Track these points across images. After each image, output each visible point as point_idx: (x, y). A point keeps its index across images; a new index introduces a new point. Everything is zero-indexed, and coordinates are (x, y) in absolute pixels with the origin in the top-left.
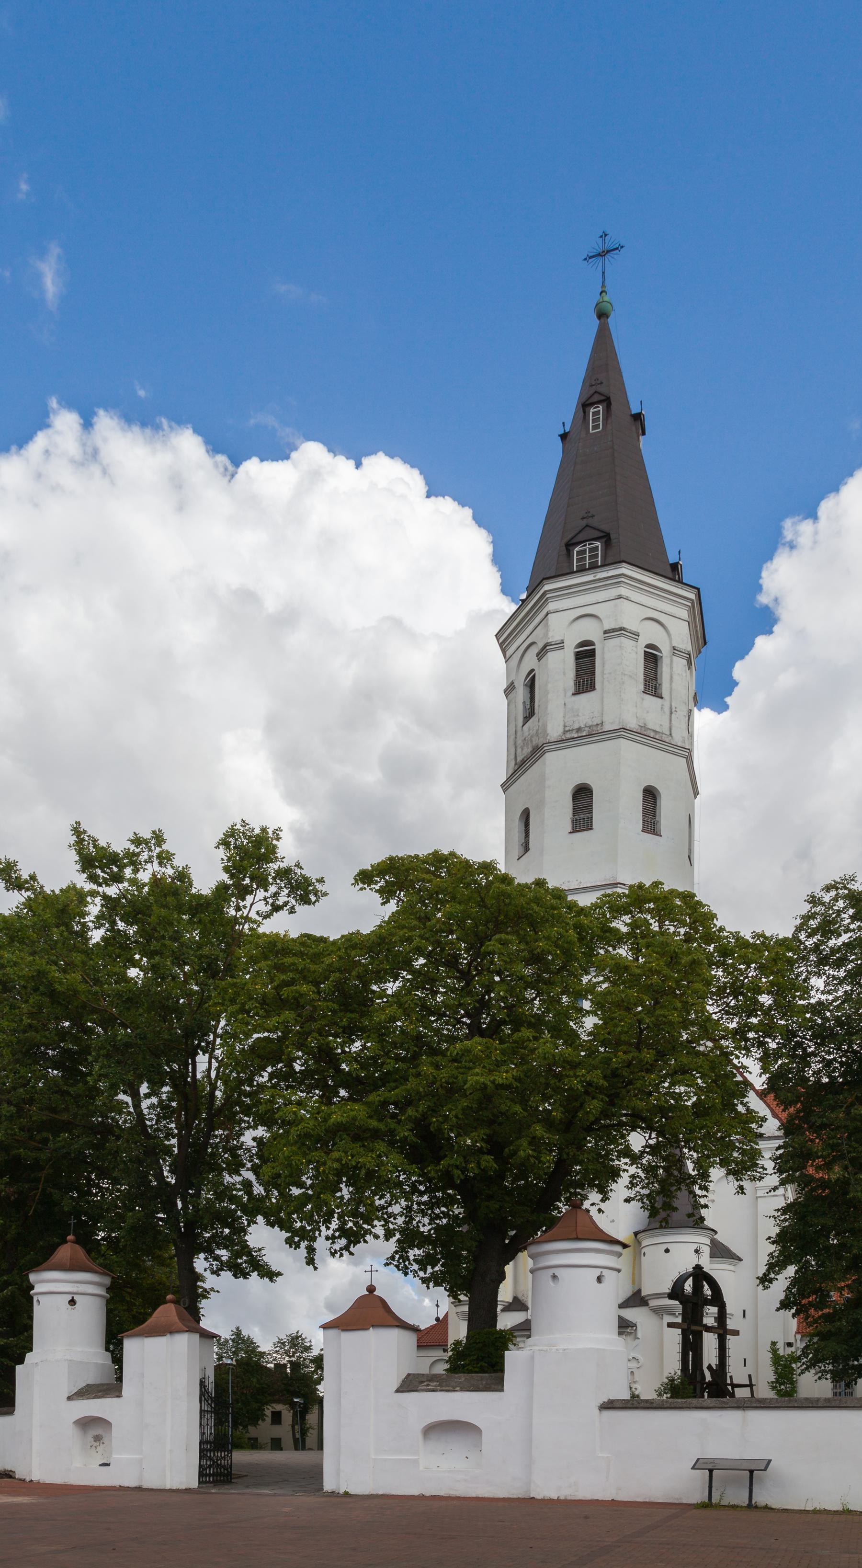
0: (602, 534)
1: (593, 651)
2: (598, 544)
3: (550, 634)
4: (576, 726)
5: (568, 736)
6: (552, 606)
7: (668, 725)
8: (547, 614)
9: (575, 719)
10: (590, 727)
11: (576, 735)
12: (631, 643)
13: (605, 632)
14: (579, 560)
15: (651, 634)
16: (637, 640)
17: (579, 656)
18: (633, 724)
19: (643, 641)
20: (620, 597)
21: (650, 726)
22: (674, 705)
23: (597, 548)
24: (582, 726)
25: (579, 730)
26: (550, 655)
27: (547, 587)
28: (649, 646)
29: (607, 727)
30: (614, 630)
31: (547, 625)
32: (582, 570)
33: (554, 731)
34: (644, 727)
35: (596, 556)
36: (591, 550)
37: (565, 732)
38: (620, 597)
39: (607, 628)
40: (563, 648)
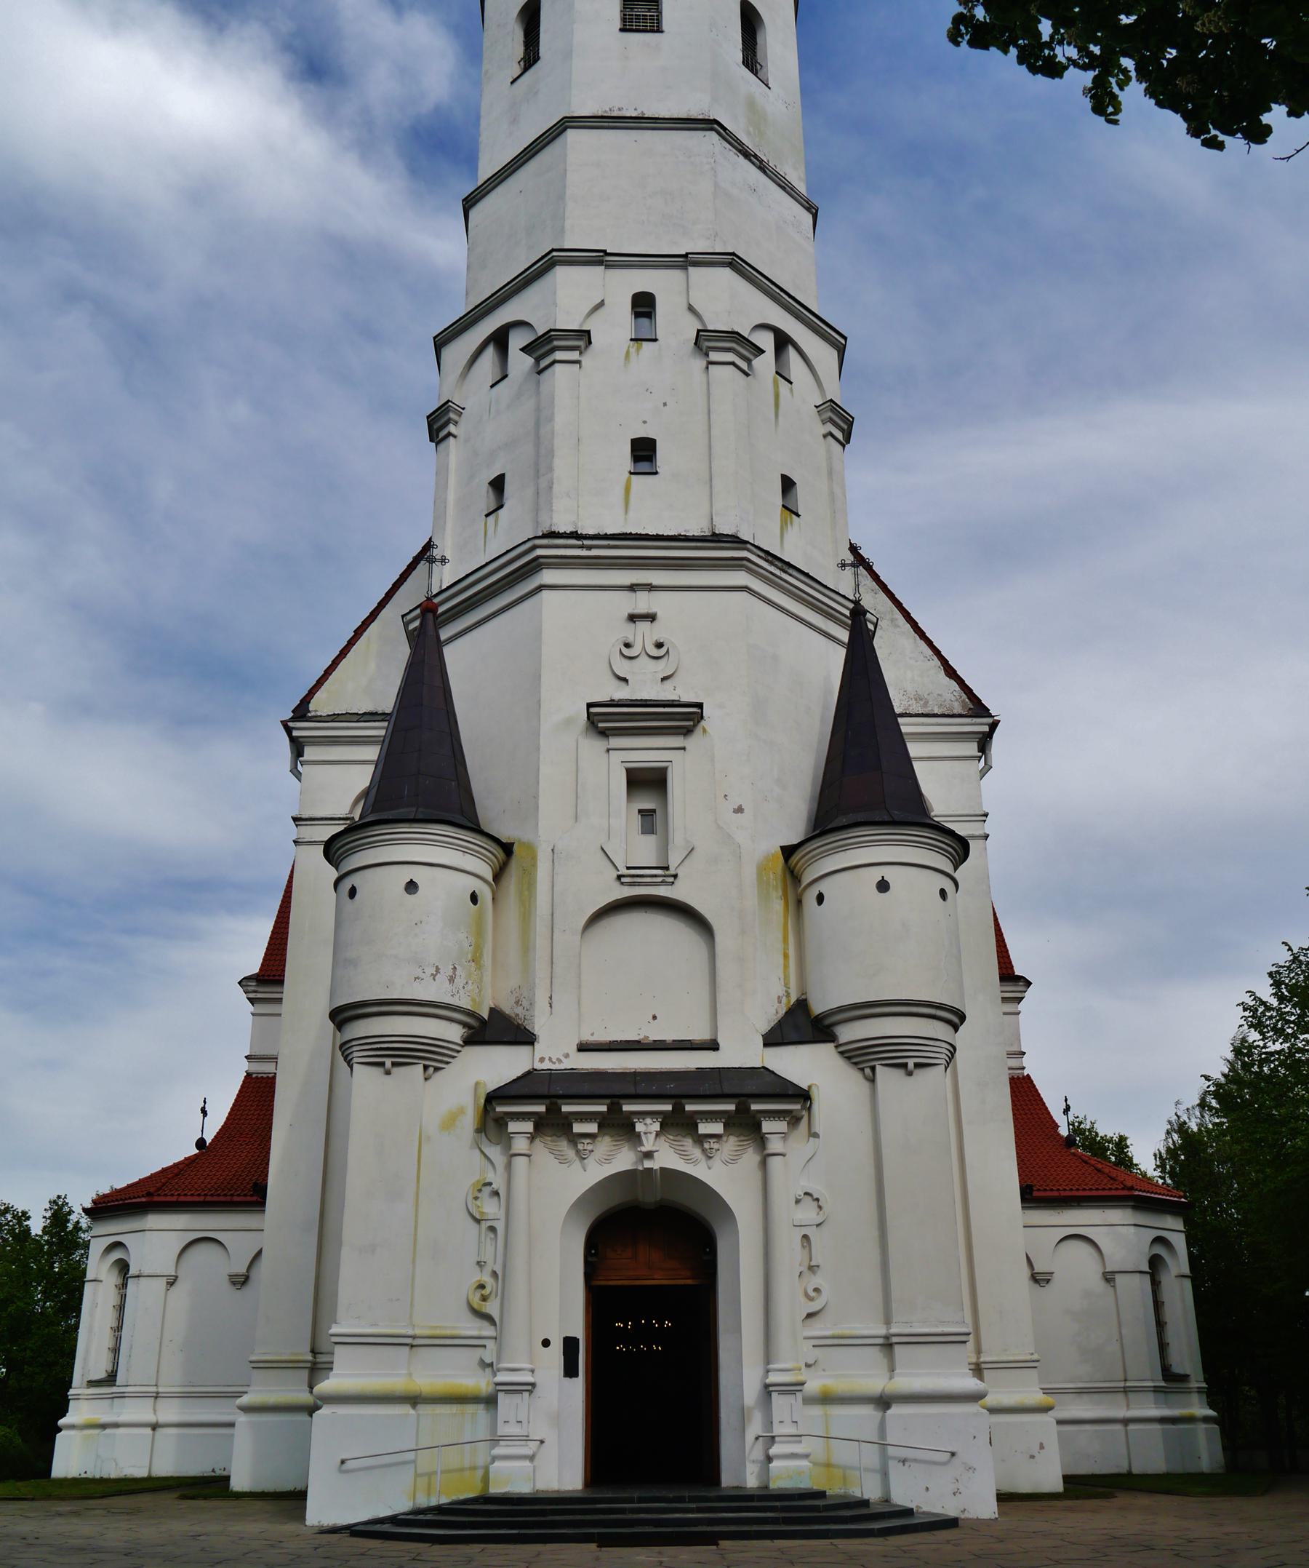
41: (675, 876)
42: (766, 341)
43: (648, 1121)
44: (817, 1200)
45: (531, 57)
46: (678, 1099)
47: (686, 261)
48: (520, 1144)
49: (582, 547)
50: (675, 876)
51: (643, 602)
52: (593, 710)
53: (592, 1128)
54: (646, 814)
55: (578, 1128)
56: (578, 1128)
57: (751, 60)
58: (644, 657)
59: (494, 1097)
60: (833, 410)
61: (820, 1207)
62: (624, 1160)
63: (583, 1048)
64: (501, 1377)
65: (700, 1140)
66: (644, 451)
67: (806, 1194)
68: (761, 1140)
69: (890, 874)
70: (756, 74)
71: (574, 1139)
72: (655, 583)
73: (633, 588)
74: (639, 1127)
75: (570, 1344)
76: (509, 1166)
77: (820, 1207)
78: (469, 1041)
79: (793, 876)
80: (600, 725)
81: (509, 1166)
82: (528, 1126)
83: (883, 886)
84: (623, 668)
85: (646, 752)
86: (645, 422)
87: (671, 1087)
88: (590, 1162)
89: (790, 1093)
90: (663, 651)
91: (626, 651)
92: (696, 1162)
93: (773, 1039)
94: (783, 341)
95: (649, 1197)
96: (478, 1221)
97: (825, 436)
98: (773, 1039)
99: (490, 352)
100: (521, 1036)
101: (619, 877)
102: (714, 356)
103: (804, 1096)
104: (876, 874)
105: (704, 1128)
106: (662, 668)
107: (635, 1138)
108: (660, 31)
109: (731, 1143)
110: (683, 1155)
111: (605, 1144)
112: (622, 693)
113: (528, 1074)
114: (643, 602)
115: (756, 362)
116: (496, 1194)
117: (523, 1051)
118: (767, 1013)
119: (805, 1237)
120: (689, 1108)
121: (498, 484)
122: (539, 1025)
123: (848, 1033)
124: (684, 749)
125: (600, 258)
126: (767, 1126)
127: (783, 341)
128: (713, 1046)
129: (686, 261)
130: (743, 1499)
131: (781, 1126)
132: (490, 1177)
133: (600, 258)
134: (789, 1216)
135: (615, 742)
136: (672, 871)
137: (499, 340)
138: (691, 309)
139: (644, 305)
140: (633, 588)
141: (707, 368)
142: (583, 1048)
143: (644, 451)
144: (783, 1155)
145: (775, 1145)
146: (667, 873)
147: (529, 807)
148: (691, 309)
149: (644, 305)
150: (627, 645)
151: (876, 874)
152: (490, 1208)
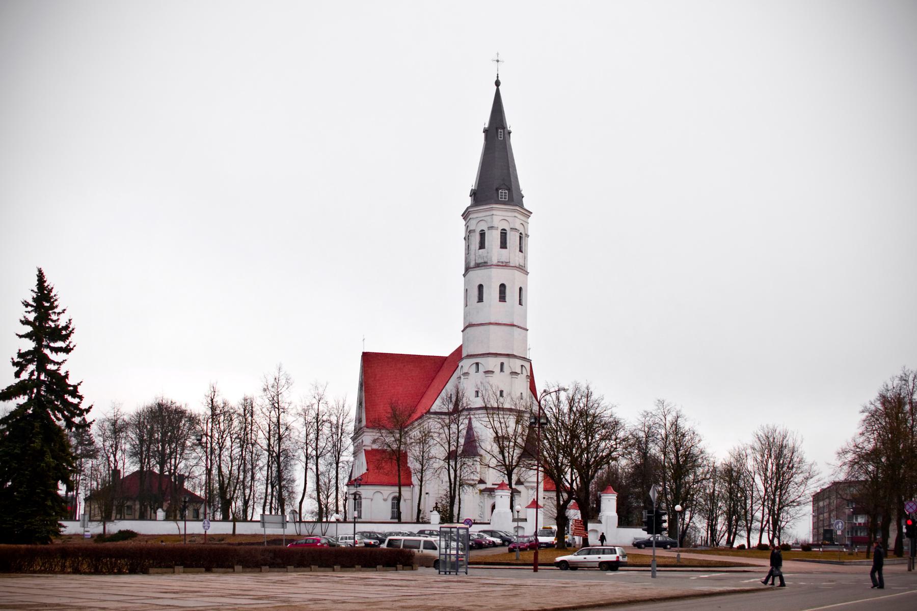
1: (506, 233)
3: (493, 223)
5: (499, 264)
6: (494, 212)
8: (493, 215)
10: (506, 262)
12: (517, 233)
13: (511, 229)
17: (501, 233)
18: (517, 265)
19: (520, 232)
20: (515, 217)
21: (521, 264)
25: (502, 262)
29: (511, 265)
30: (514, 229)
31: (492, 218)
33: (495, 261)
37: (498, 262)
38: (515, 217)
39: (511, 227)
48: (486, 497)
63: (493, 484)
78: (478, 483)
94: (522, 366)
99: (475, 365)
100: (485, 483)
102: (513, 376)
103: (520, 492)
108: (505, 301)
113: (486, 488)
117: (485, 485)
122: (487, 481)
127: (522, 366)
129: (508, 355)
139: (502, 364)
142: (493, 484)
149: (502, 364)
152: (481, 504)
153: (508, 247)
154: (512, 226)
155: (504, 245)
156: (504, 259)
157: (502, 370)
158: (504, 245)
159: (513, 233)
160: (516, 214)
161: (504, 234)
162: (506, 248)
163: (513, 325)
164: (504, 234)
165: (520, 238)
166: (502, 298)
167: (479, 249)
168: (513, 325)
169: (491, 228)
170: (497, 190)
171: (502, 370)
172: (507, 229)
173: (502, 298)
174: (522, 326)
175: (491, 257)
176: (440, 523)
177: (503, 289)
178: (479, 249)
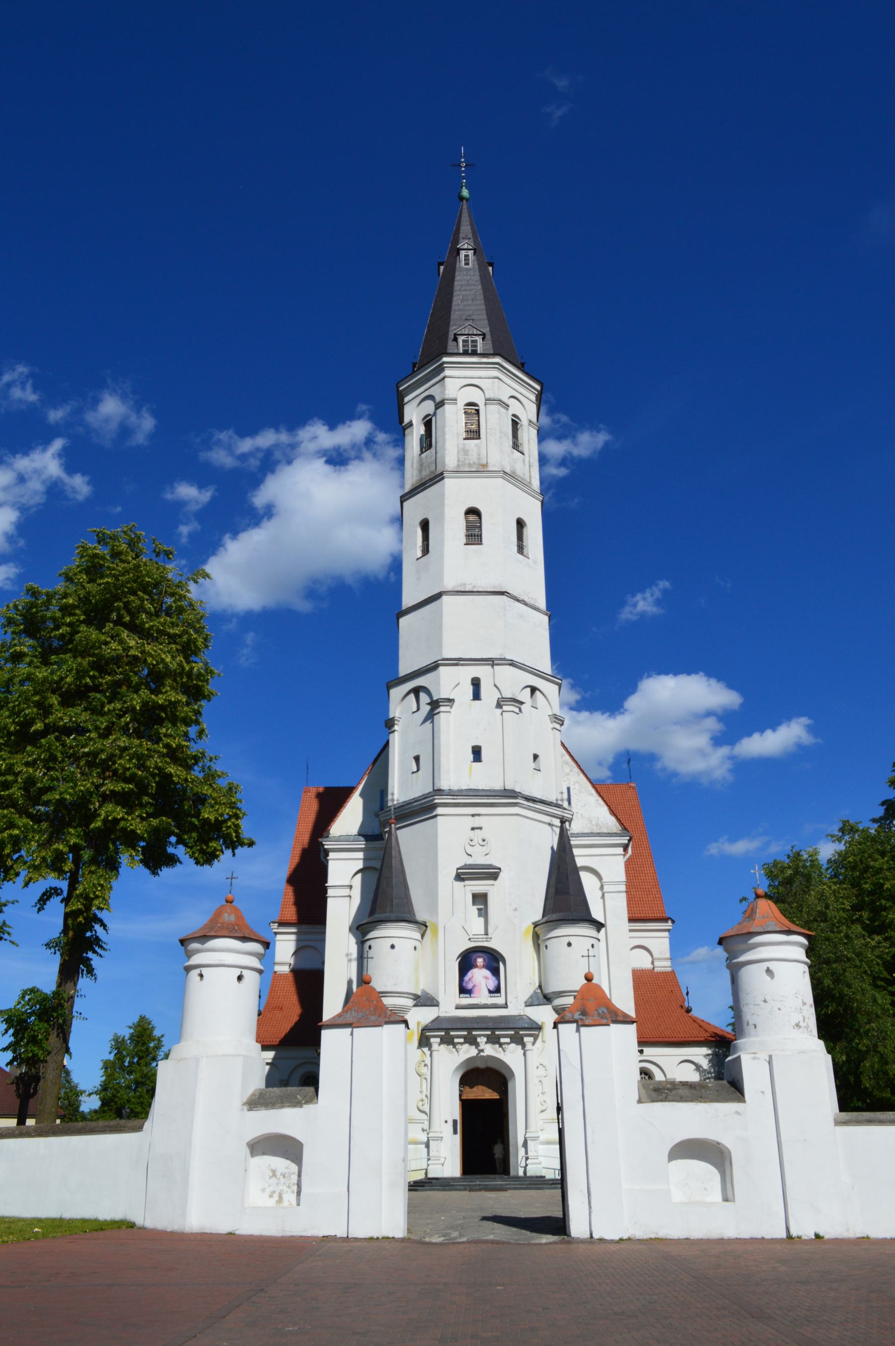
0: (480, 333)
1: (478, 411)
2: (477, 338)
3: (447, 392)
4: (467, 462)
5: (462, 469)
7: (528, 475)
9: (466, 457)
11: (467, 470)
14: (464, 346)
15: (515, 408)
16: (507, 410)
18: (508, 470)
19: (511, 411)
22: (531, 461)
23: (476, 341)
24: (471, 462)
26: (447, 407)
27: (445, 359)
28: (514, 415)
31: (444, 386)
32: (466, 353)
34: (514, 472)
35: (476, 346)
36: (473, 341)
37: (458, 466)
39: (487, 396)
40: (456, 404)
41: (491, 938)
42: (525, 696)
43: (482, 1037)
44: (545, 1067)
45: (426, 550)
46: (493, 1029)
47: (492, 662)
48: (435, 1046)
49: (453, 799)
50: (491, 938)
51: (477, 822)
52: (459, 871)
53: (462, 1040)
54: (479, 910)
55: (456, 1040)
56: (456, 1040)
57: (521, 549)
58: (478, 845)
59: (425, 1029)
60: (556, 718)
61: (546, 1070)
62: (472, 1052)
64: (430, 1135)
65: (501, 1045)
66: (477, 753)
67: (541, 1064)
68: (524, 1046)
69: (572, 940)
70: (523, 555)
71: (454, 1045)
72: (482, 813)
73: (473, 815)
74: (479, 1040)
75: (455, 1122)
76: (431, 1055)
77: (546, 1070)
78: (415, 1006)
79: (536, 937)
80: (462, 876)
81: (431, 1055)
82: (438, 1040)
83: (569, 944)
84: (470, 850)
85: (479, 886)
86: (477, 738)
87: (490, 1025)
88: (461, 1052)
89: (534, 1027)
90: (486, 842)
91: (471, 843)
92: (500, 1052)
93: (529, 1004)
94: (533, 690)
95: (481, 1065)
96: (420, 1076)
97: (552, 729)
98: (529, 1004)
99: (412, 696)
101: (469, 939)
104: (567, 940)
105: (502, 1040)
106: (484, 850)
107: (477, 1045)
109: (513, 1045)
110: (495, 1050)
111: (466, 1046)
112: (470, 861)
113: (438, 1019)
114: (477, 822)
115: (523, 707)
116: (426, 1065)
118: (526, 995)
119: (540, 1081)
120: (497, 1033)
121: (417, 759)
122: (441, 998)
123: (558, 1002)
124: (493, 885)
125: (457, 662)
126: (526, 1039)
127: (533, 690)
128: (505, 1006)
129: (492, 662)
130: (517, 1178)
131: (531, 1039)
132: (425, 1059)
133: (457, 662)
134: (533, 1073)
135: (467, 882)
136: (489, 936)
137: (416, 691)
138: (495, 685)
139: (476, 683)
140: (473, 815)
141: (502, 714)
143: (477, 753)
144: (532, 1050)
145: (529, 1046)
146: (488, 937)
147: (433, 906)
148: (495, 685)
149: (476, 683)
150: (471, 840)
151: (567, 940)
153: (482, 436)
154: (489, 395)
155: (474, 434)
156: (473, 458)
157: (477, 696)
158: (474, 434)
159: (494, 408)
160: (495, 373)
161: (473, 410)
162: (479, 438)
163: (502, 593)
164: (473, 410)
165: (515, 424)
166: (474, 535)
167: (422, 452)
168: (502, 593)
169: (440, 405)
170: (455, 339)
171: (477, 696)
172: (481, 402)
173: (474, 535)
174: (526, 600)
175: (443, 457)
176: (256, 1102)
177: (472, 518)
178: (422, 452)
